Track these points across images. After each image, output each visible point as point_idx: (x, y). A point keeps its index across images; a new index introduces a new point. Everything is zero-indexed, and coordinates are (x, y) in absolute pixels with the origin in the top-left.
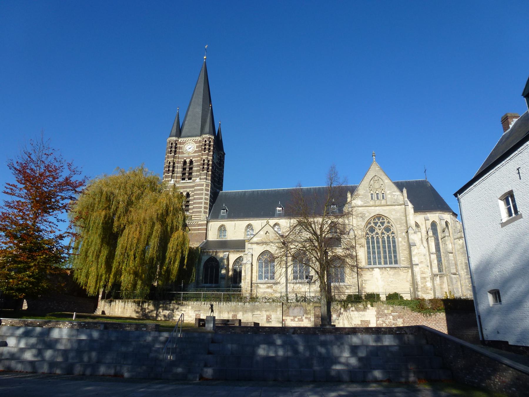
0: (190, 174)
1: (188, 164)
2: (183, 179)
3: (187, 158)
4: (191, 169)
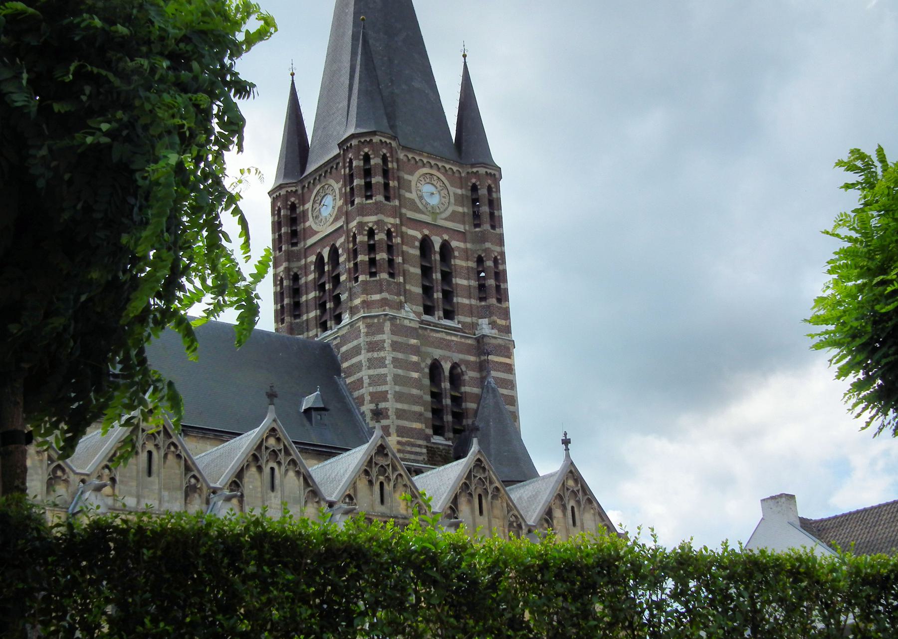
0: (448, 295)
2: (429, 310)
4: (447, 277)
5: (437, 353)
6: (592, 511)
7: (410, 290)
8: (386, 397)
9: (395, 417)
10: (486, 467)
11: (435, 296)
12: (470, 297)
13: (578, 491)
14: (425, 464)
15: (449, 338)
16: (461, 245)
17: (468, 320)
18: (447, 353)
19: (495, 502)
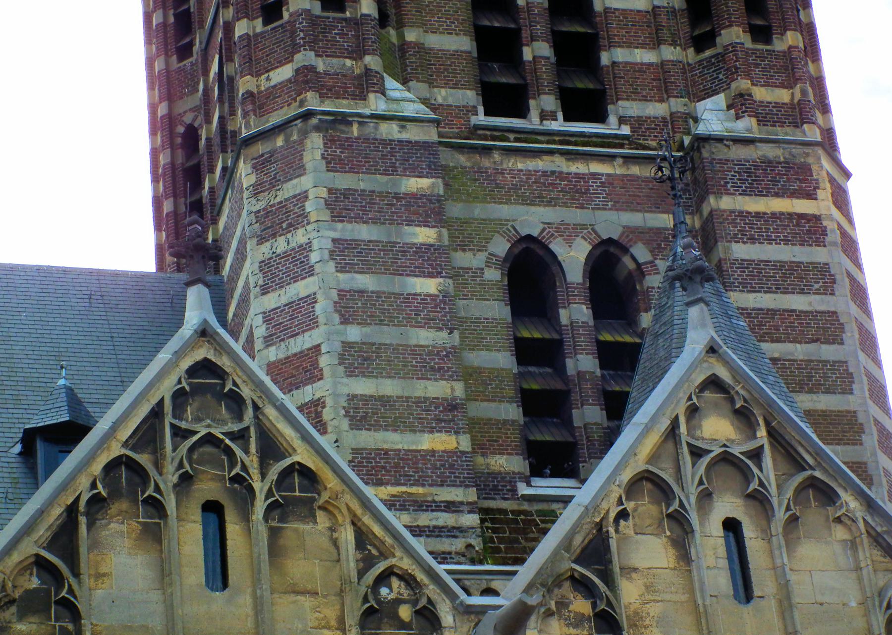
6: (840, 533)
7: (419, 46)
8: (315, 364)
9: (345, 424)
10: (246, 392)
11: (527, 54)
12: (656, 43)
13: (756, 455)
14: (473, 562)
15: (578, 167)
17: (657, 109)
18: (575, 215)
19: (295, 527)
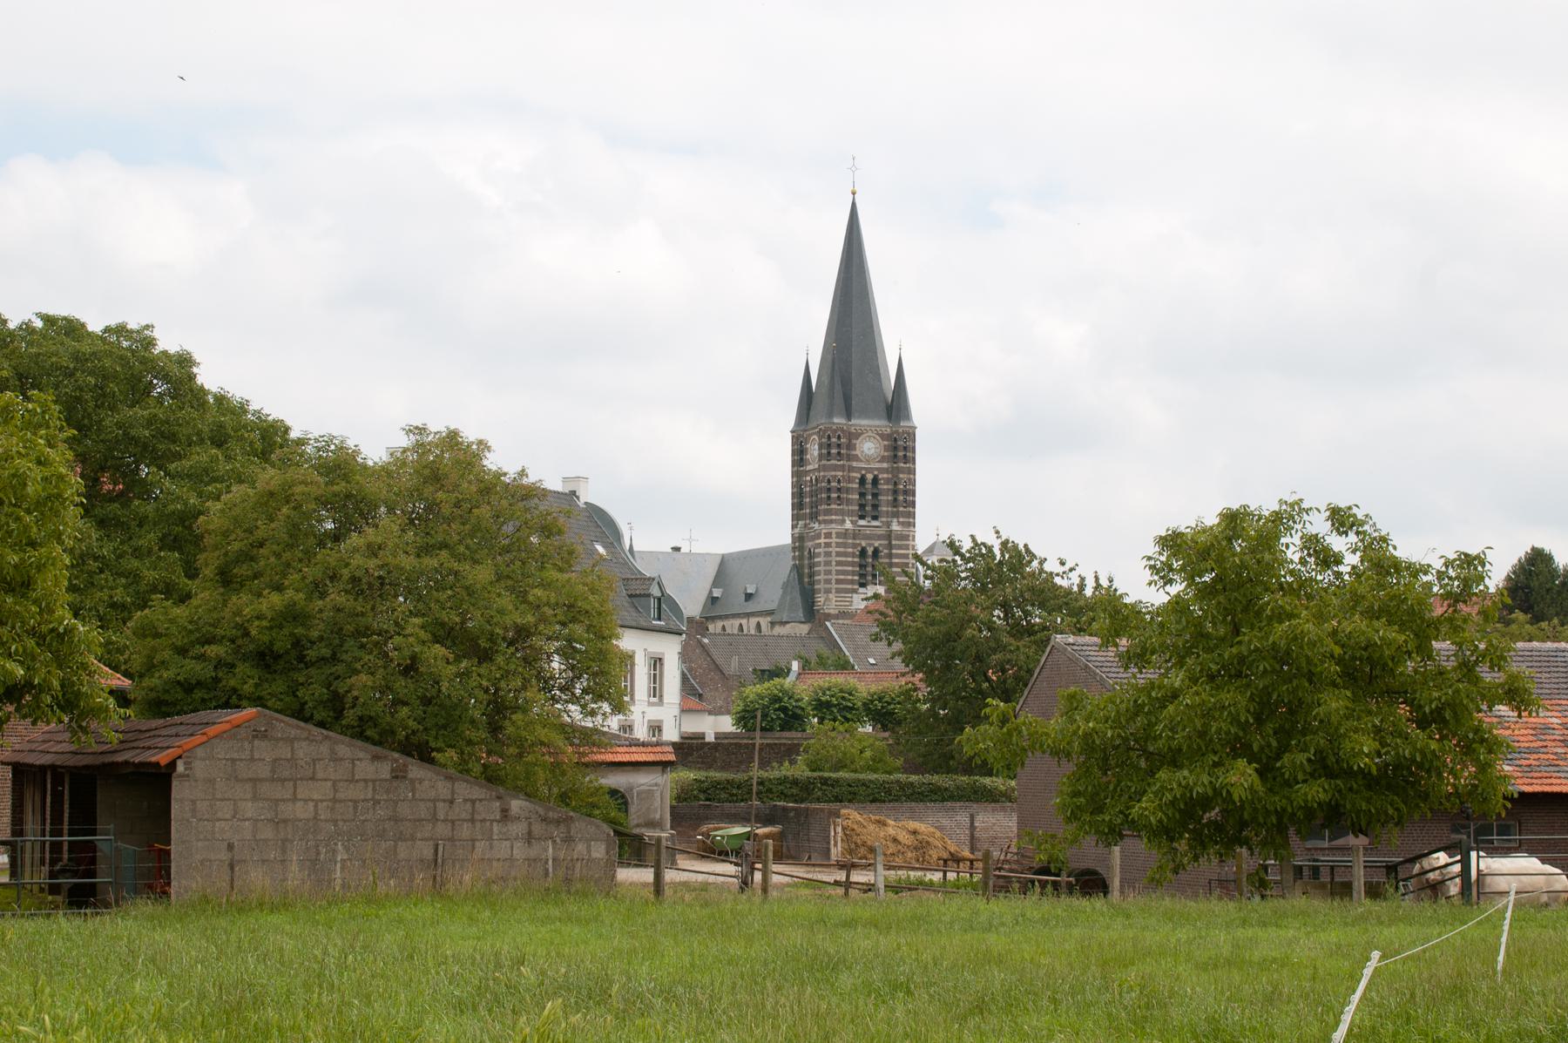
0: (875, 507)
1: (869, 486)
2: (862, 517)
3: (869, 470)
4: (875, 495)
5: (864, 545)
16: (885, 476)
